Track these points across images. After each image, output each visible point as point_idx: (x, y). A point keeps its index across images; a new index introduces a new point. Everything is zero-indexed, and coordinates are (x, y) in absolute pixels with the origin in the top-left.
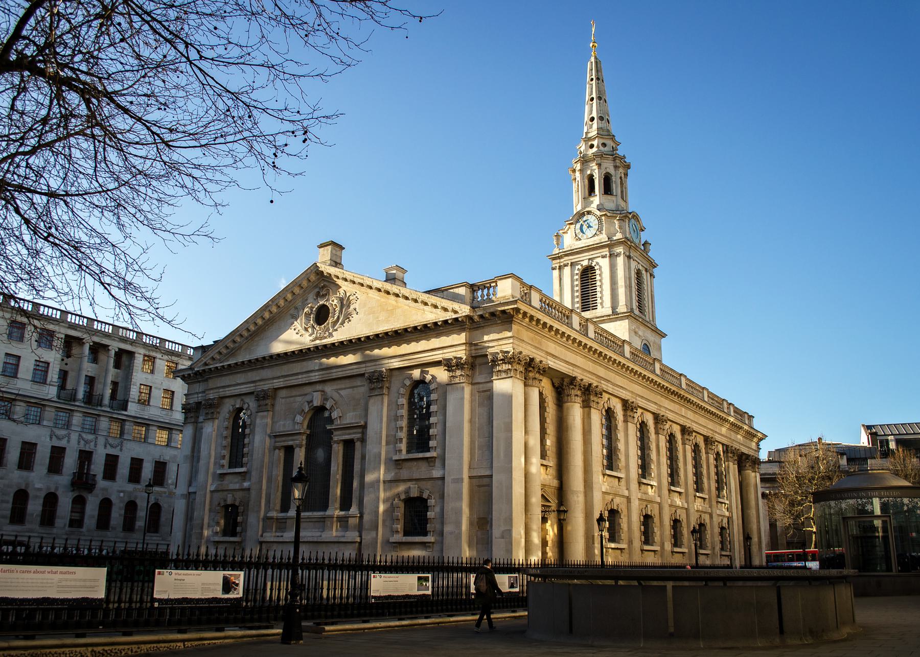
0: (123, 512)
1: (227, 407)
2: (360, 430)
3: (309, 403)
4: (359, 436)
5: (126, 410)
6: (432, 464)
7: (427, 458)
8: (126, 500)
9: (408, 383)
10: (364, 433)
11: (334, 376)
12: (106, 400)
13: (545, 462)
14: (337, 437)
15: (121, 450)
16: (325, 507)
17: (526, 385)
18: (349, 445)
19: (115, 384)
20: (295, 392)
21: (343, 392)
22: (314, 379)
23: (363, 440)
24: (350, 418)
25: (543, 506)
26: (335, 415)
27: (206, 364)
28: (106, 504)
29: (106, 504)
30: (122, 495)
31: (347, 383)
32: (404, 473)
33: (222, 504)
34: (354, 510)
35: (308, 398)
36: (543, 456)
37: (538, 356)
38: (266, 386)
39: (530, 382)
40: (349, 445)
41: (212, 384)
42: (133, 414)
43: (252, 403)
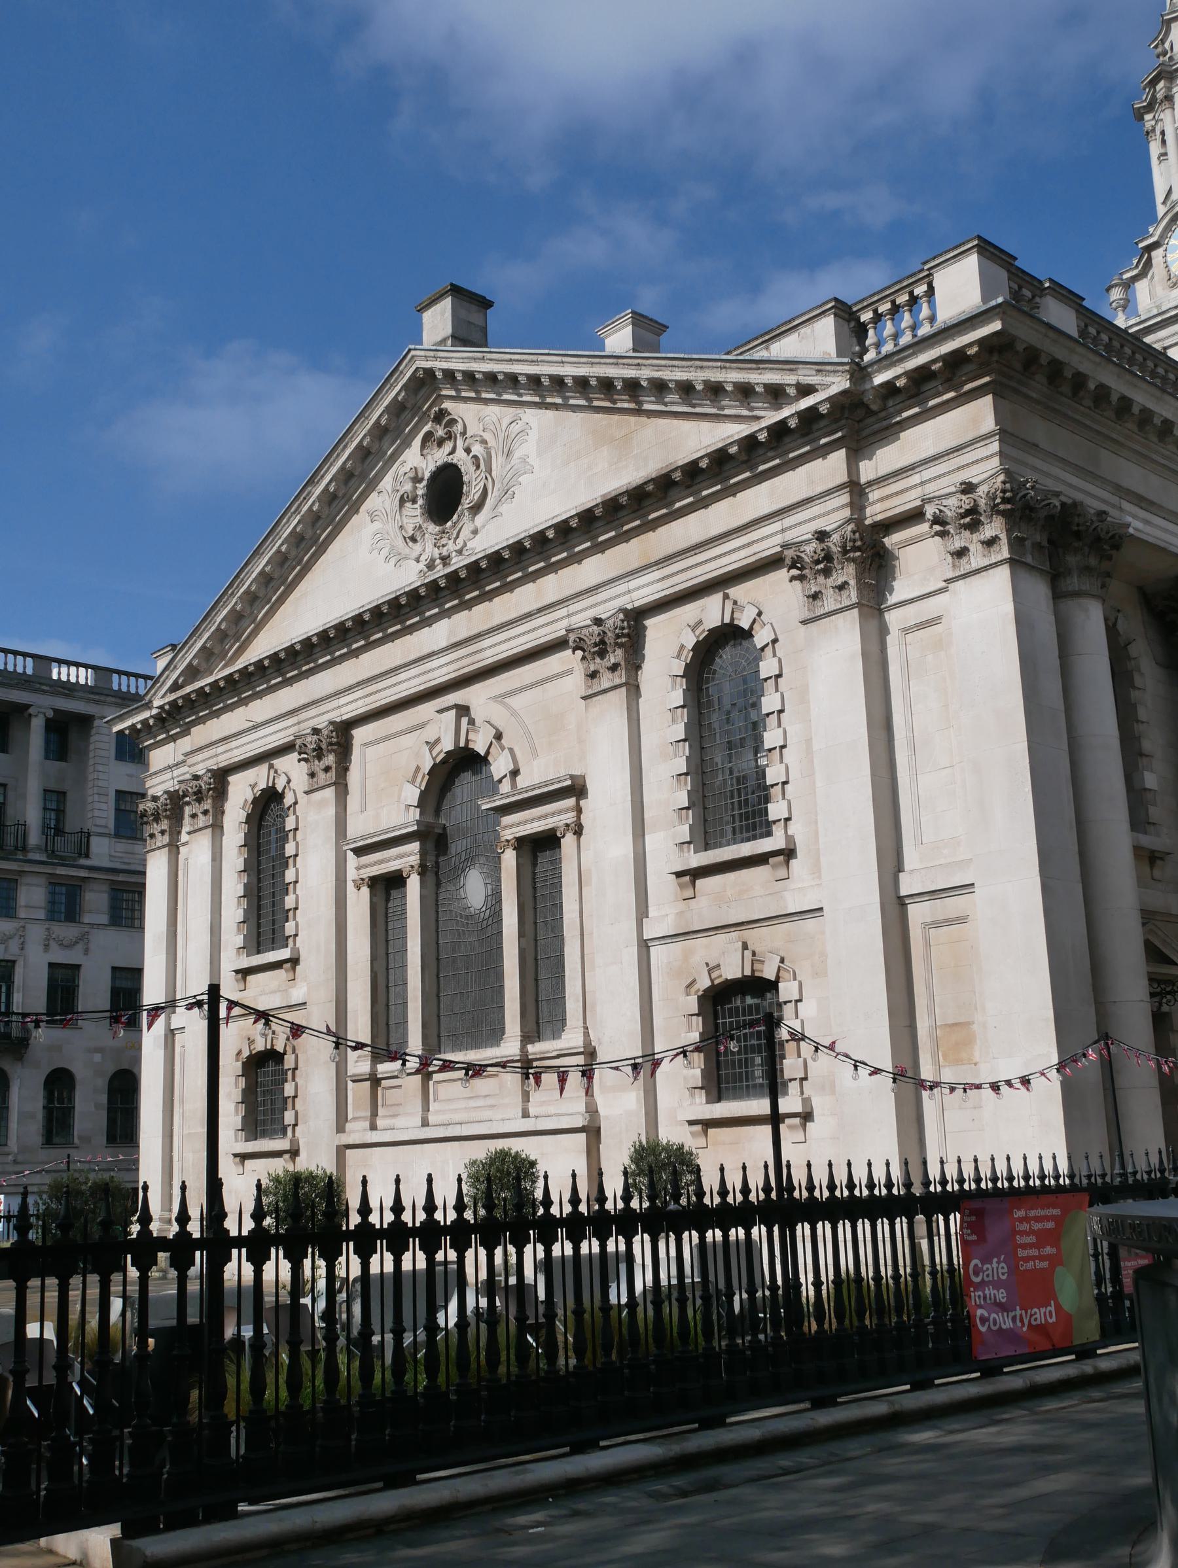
0: (104, 1099)
2: (571, 802)
3: (431, 745)
4: (570, 817)
5: (87, 856)
7: (760, 860)
8: (111, 1069)
9: (690, 641)
10: (579, 811)
12: (34, 838)
13: (1146, 841)
15: (86, 951)
16: (496, 1034)
17: (1058, 596)
19: (56, 801)
21: (516, 702)
23: (578, 831)
24: (537, 774)
25: (1152, 979)
26: (499, 766)
28: (60, 1083)
29: (60, 1083)
30: (97, 1057)
34: (572, 1038)
35: (430, 734)
36: (1139, 821)
37: (1092, 498)
38: (322, 718)
39: (1073, 583)
42: (106, 863)
43: (292, 769)
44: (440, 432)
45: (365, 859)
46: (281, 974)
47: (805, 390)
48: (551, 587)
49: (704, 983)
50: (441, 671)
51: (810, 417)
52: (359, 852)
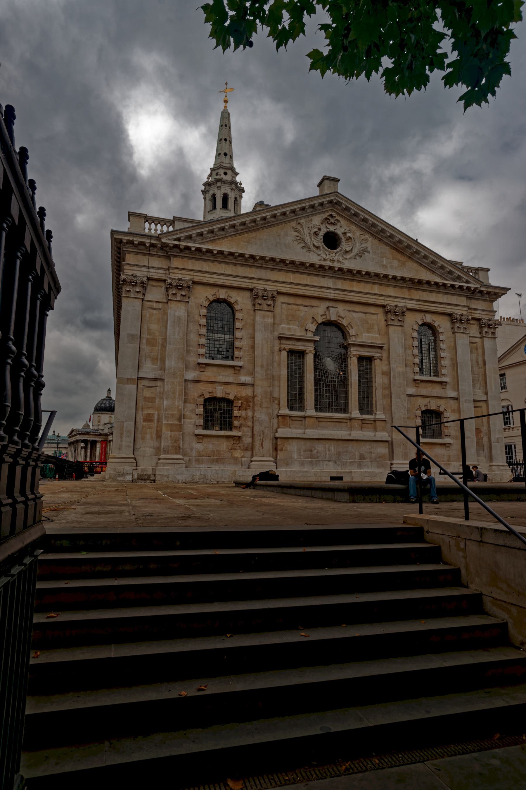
2: (379, 351)
4: (379, 355)
6: (444, 387)
11: (352, 297)
14: (355, 352)
18: (366, 361)
20: (299, 301)
21: (355, 315)
22: (328, 296)
24: (365, 338)
27: (179, 239)
32: (424, 390)
38: (271, 288)
40: (366, 361)
41: (176, 263)
44: (332, 221)
45: (283, 342)
46: (231, 371)
48: (376, 289)
49: (423, 409)
51: (468, 288)
52: (280, 338)
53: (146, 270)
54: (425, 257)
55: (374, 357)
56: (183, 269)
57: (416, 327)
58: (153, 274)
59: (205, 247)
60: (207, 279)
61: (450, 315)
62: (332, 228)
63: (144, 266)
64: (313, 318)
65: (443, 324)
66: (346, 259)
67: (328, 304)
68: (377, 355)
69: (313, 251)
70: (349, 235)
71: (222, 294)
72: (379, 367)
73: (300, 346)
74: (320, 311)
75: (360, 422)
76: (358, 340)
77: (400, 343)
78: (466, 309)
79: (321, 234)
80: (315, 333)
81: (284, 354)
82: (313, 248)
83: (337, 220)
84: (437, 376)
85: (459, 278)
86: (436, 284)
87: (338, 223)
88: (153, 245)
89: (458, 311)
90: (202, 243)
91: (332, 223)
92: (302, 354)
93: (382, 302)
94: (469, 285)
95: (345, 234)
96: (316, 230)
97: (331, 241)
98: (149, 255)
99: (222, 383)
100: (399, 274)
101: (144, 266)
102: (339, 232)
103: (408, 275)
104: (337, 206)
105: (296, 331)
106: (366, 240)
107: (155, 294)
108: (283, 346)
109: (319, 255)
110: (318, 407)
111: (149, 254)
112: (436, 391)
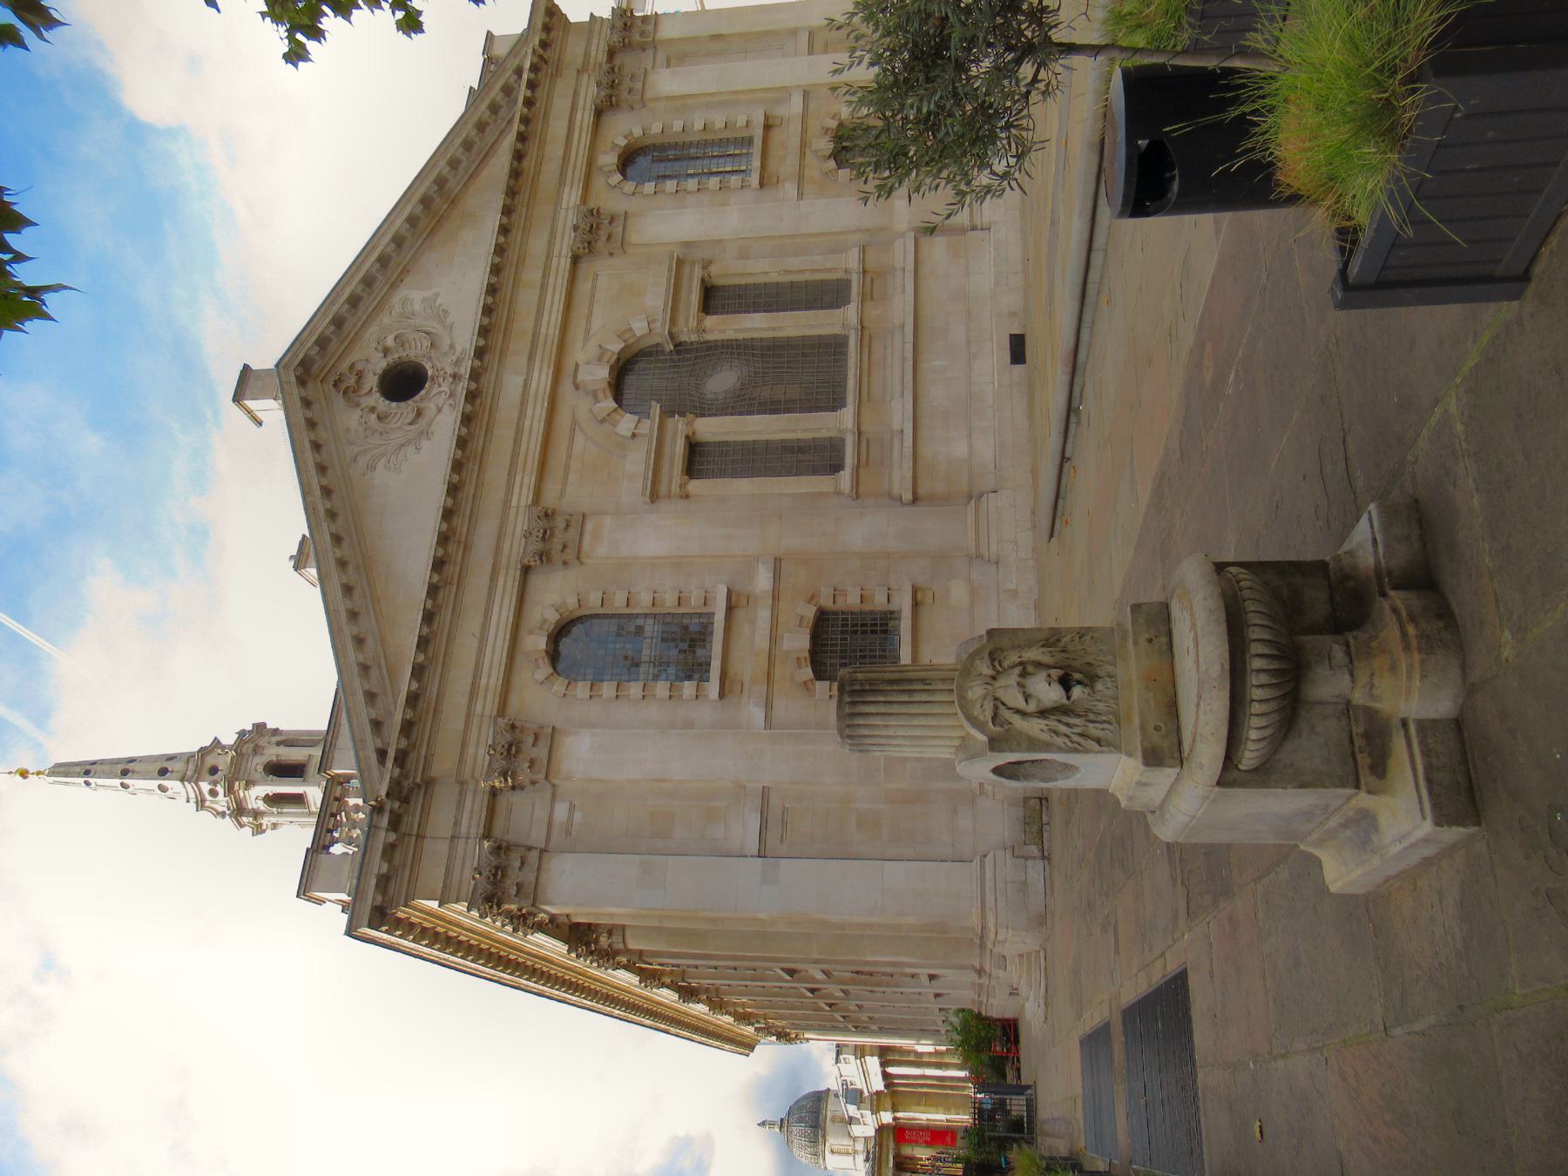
1: (539, 696)
2: (687, 269)
18: (712, 299)
21: (596, 324)
24: (655, 299)
27: (382, 754)
31: (580, 309)
33: (807, 672)
38: (520, 522)
40: (712, 299)
41: (443, 765)
44: (352, 381)
45: (663, 489)
46: (740, 615)
47: (519, 72)
50: (542, 380)
51: (534, 68)
52: (654, 497)
53: (461, 844)
54: (454, 164)
55: (703, 280)
56: (462, 742)
57: (629, 186)
58: (472, 821)
59: (405, 684)
60: (492, 679)
61: (599, 113)
62: (372, 381)
63: (452, 849)
64: (603, 421)
65: (623, 128)
66: (452, 347)
67: (566, 387)
68: (698, 273)
69: (430, 424)
70: (390, 342)
71: (537, 643)
72: (729, 271)
73: (677, 450)
74: (588, 402)
75: (868, 304)
76: (660, 318)
77: (672, 220)
78: (585, 78)
79: (383, 404)
80: (643, 414)
81: (695, 486)
82: (422, 422)
83: (352, 367)
84: (750, 141)
85: (508, 90)
86: (522, 138)
87: (359, 367)
88: (395, 824)
89: (590, 93)
90: (395, 696)
91: (358, 382)
92: (695, 450)
93: (565, 263)
94: (527, 65)
95: (386, 352)
96: (374, 417)
97: (404, 382)
98: (420, 837)
99: (770, 637)
100: (493, 220)
101: (452, 849)
102: (380, 364)
103: (498, 201)
104: (315, 368)
105: (636, 461)
106: (405, 301)
107: (526, 816)
108: (675, 489)
109: (439, 410)
110: (836, 404)
111: (418, 836)
112: (788, 138)
